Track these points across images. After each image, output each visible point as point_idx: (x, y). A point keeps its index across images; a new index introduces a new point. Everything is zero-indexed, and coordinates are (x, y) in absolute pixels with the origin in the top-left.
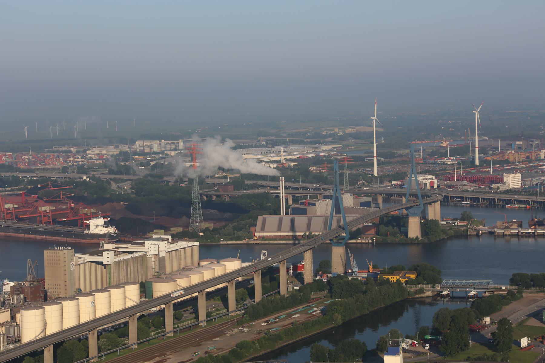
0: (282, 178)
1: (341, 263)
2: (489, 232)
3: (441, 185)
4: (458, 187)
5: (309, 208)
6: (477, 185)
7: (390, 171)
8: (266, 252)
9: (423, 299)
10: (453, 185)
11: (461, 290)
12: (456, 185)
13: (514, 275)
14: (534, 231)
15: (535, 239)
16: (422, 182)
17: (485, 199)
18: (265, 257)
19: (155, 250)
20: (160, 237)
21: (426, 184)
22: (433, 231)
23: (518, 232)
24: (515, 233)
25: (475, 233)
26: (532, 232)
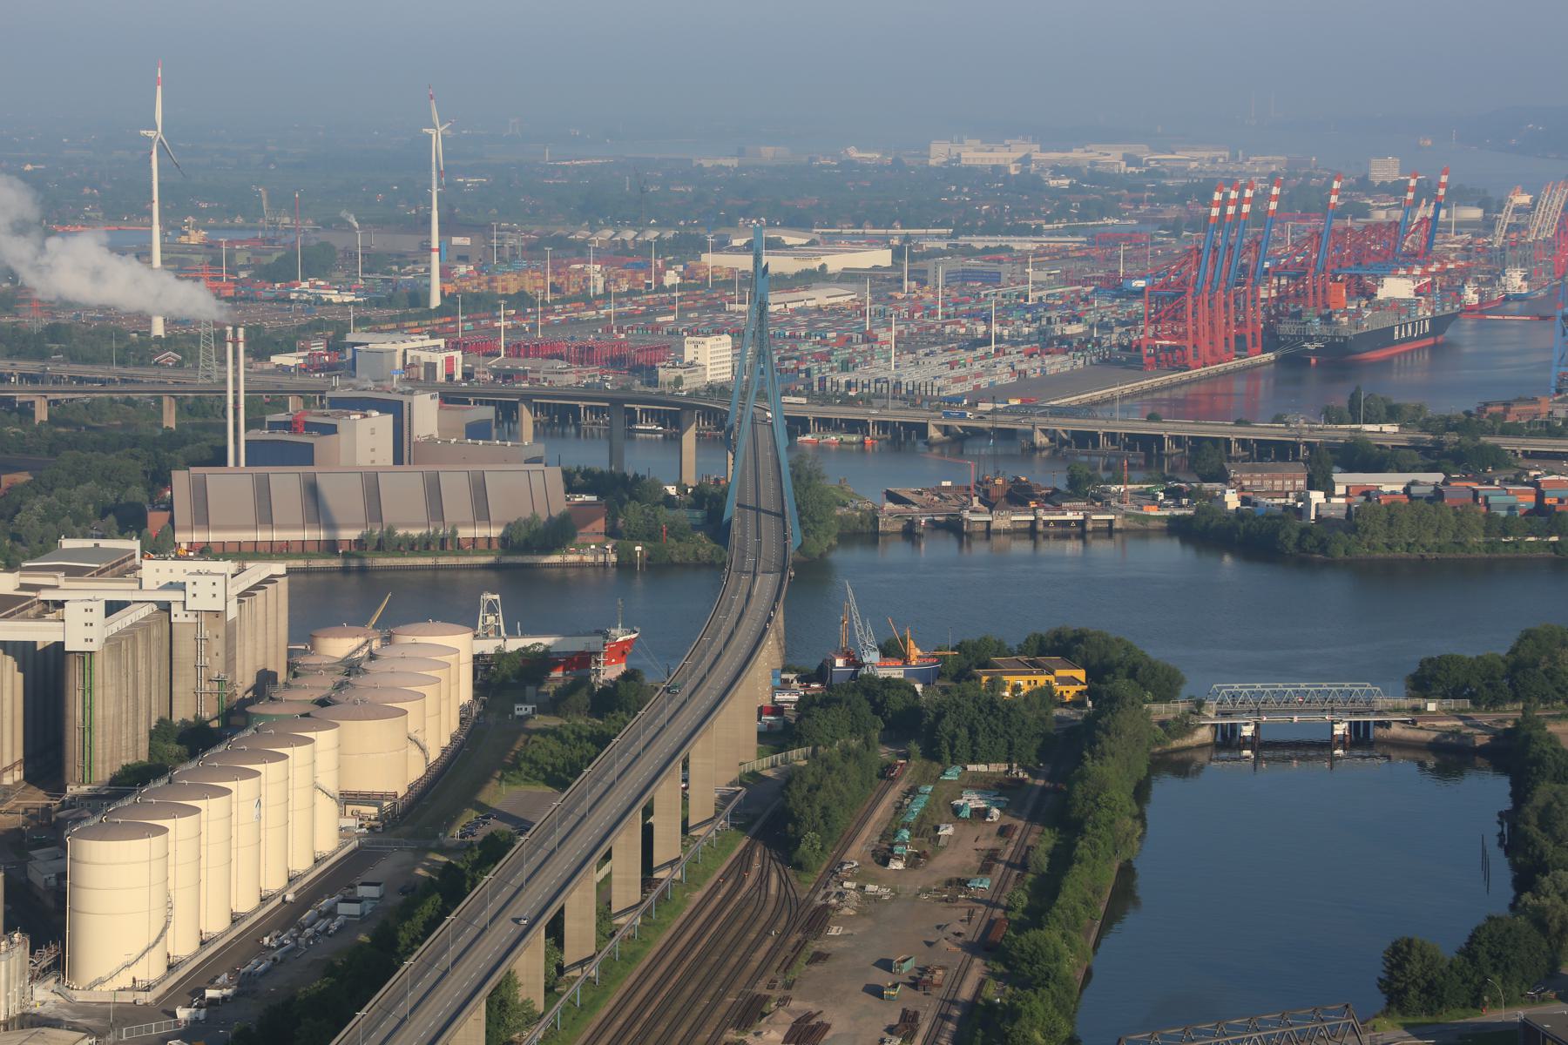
0: (235, 332)
3: (477, 369)
4: (541, 376)
5: (320, 442)
6: (596, 370)
8: (497, 597)
12: (531, 371)
14: (1081, 518)
15: (1085, 542)
16: (419, 358)
17: (650, 413)
18: (493, 618)
19: (214, 595)
20: (96, 545)
21: (434, 365)
22: (817, 519)
23: (1033, 523)
24: (1022, 526)
25: (899, 526)
26: (1075, 521)
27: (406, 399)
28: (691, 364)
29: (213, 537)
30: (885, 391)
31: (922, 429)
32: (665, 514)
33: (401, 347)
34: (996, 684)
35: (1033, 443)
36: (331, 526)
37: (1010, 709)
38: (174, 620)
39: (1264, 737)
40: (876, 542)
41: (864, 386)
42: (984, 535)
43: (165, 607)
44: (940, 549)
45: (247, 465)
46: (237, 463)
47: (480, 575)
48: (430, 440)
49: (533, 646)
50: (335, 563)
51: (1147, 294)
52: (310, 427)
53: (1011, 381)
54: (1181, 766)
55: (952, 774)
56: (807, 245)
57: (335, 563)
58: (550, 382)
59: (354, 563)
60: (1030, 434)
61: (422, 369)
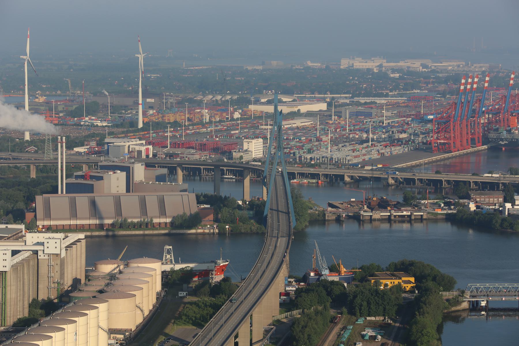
0: (62, 139)
3: (158, 153)
4: (185, 156)
5: (96, 184)
6: (207, 153)
8: (171, 247)
10: (177, 153)
12: (181, 154)
14: (409, 214)
15: (411, 224)
16: (135, 148)
17: (230, 171)
18: (169, 256)
19: (56, 247)
20: (7, 227)
22: (300, 214)
24: (385, 217)
25: (334, 217)
26: (407, 215)
27: (131, 166)
28: (246, 151)
29: (53, 223)
30: (326, 161)
31: (342, 177)
32: (238, 213)
33: (127, 144)
34: (377, 284)
35: (388, 183)
36: (101, 218)
37: (384, 294)
38: (39, 258)
39: (490, 306)
40: (324, 224)
41: (317, 159)
42: (369, 221)
43: (36, 252)
44: (351, 227)
45: (66, 193)
46: (62, 192)
47: (162, 238)
48: (141, 182)
49: (186, 267)
50: (103, 233)
51: (434, 121)
52: (92, 177)
53: (378, 157)
54: (455, 318)
55: (361, 321)
56: (292, 101)
57: (103, 233)
58: (188, 158)
59: (110, 233)
60: (387, 179)
61: (136, 153)
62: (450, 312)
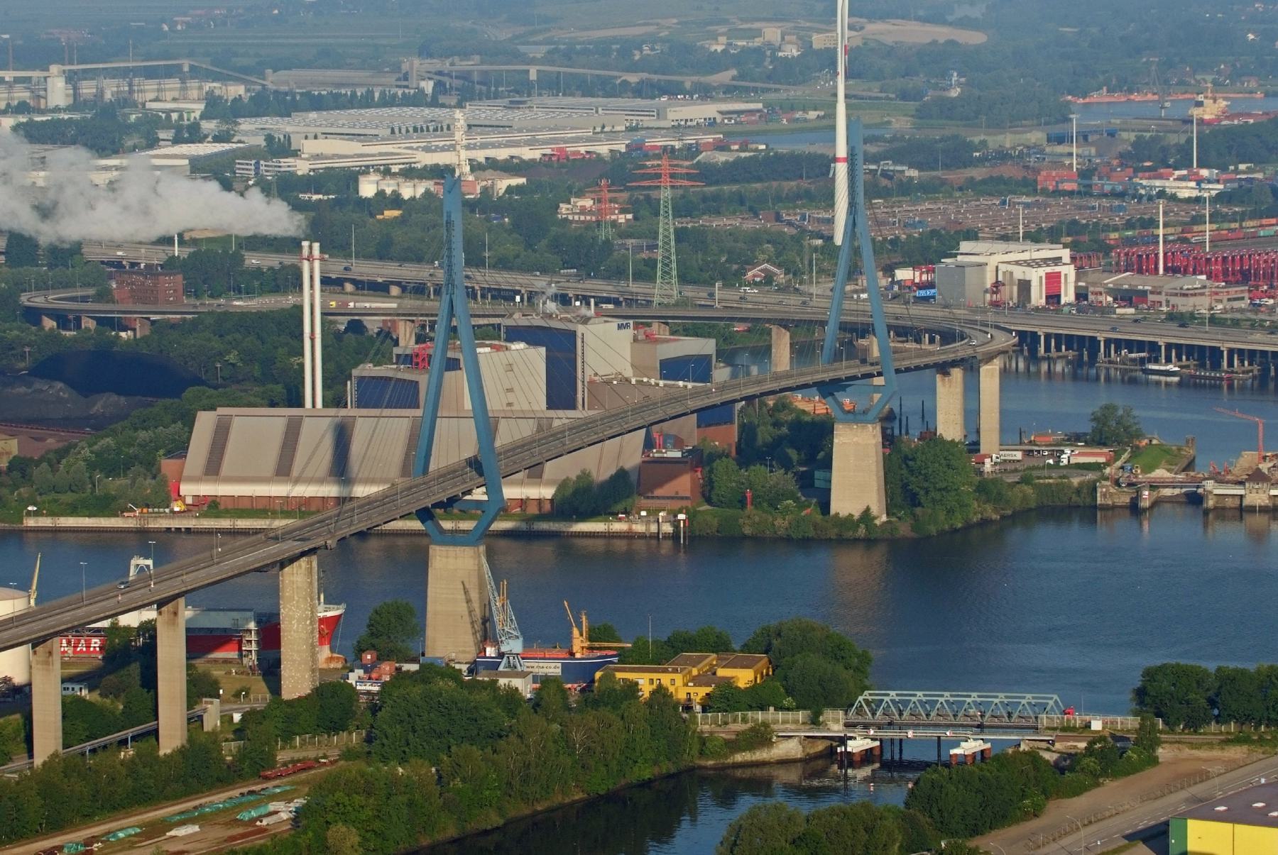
0: (311, 247)
1: (467, 619)
2: (1187, 494)
3: (1091, 289)
4: (1162, 298)
6: (1242, 291)
7: (914, 226)
8: (150, 562)
9: (765, 771)
10: (1140, 291)
11: (921, 733)
13: (1150, 674)
16: (1011, 273)
25: (1126, 499)
27: (580, 329)
40: (1093, 521)
42: (1238, 513)
45: (324, 406)
58: (1173, 306)
61: (1015, 289)
62: (725, 767)
